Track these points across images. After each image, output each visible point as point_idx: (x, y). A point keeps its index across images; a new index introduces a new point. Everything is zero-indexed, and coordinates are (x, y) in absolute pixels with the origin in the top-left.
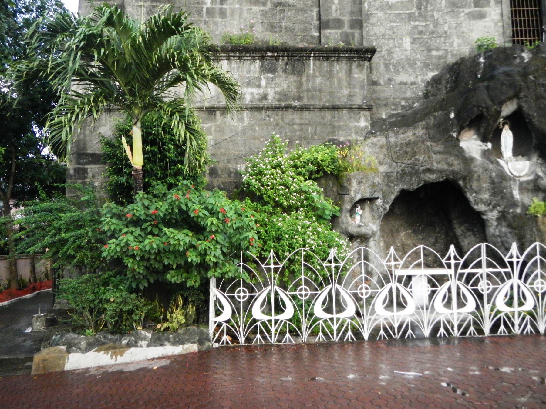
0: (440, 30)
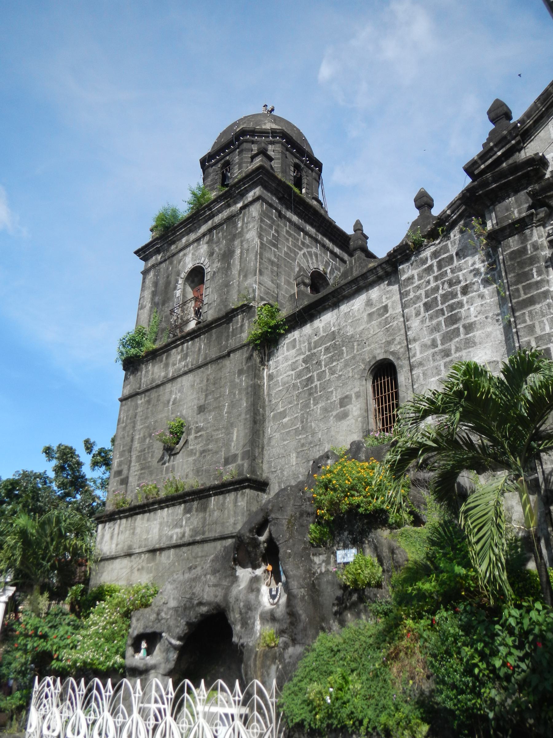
0: (316, 439)
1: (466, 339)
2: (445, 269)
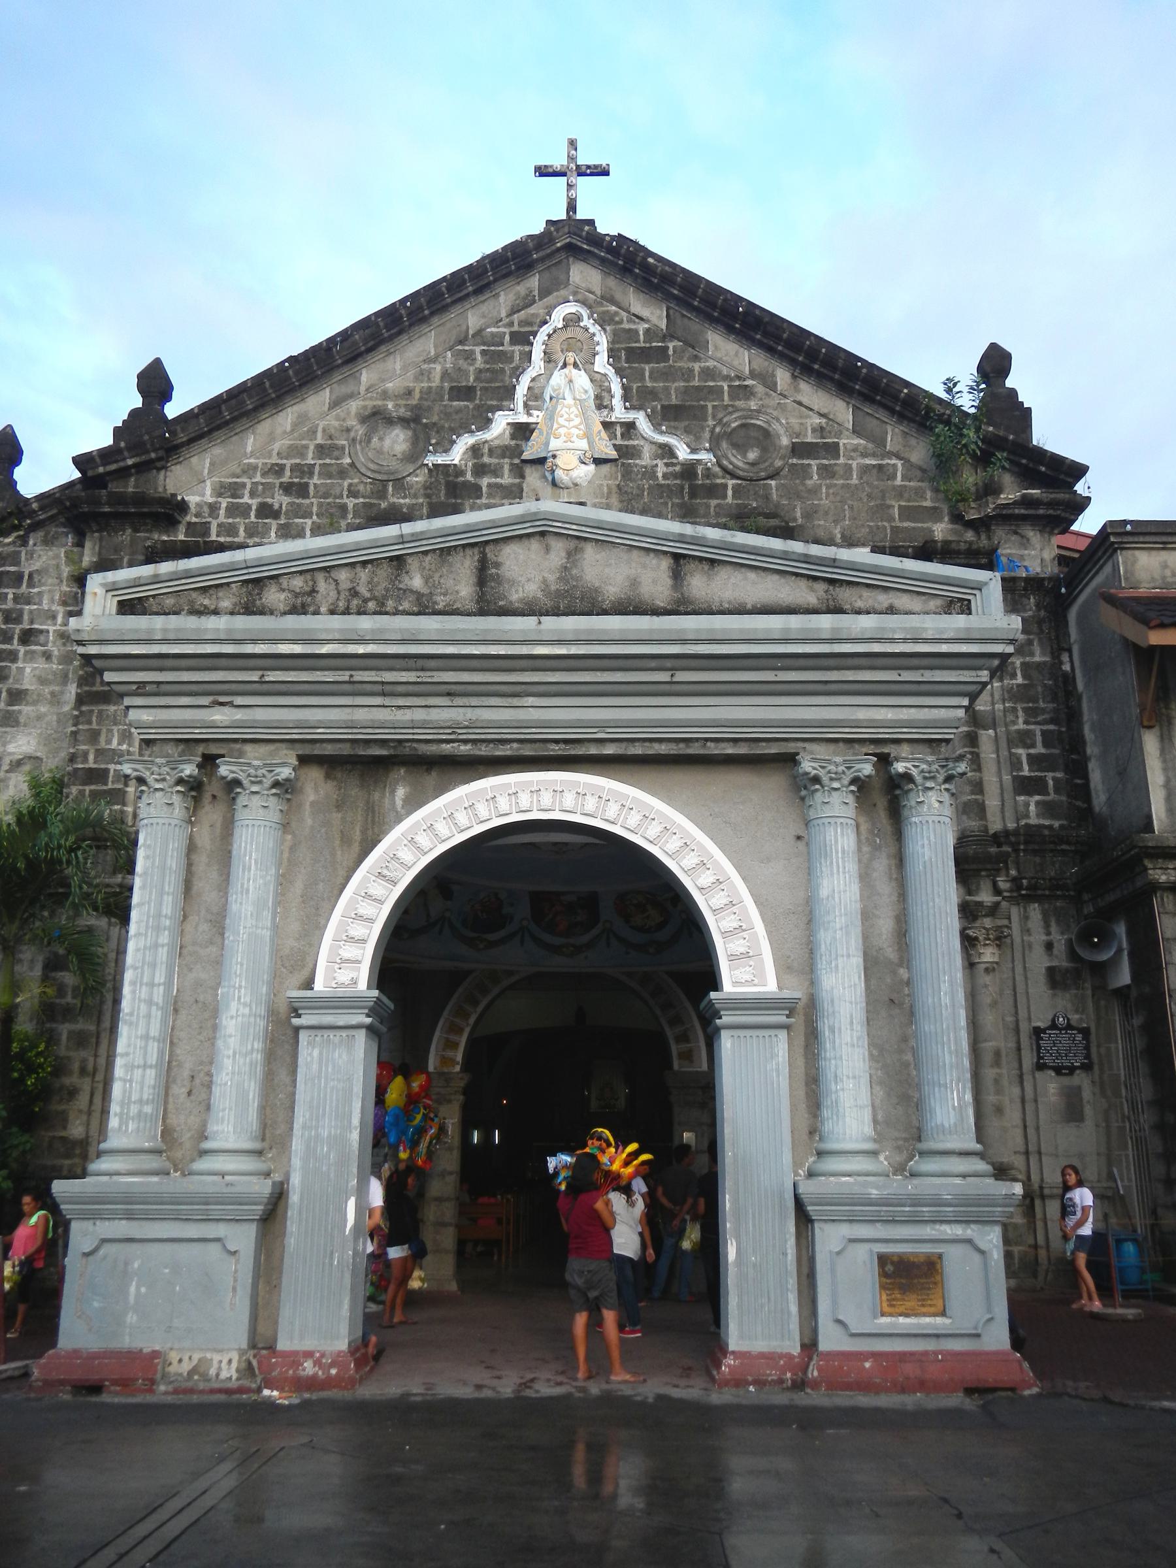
1: (8, 711)
2: (6, 590)
